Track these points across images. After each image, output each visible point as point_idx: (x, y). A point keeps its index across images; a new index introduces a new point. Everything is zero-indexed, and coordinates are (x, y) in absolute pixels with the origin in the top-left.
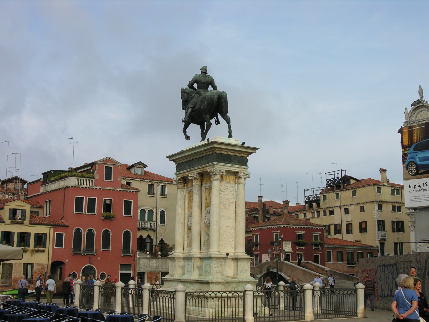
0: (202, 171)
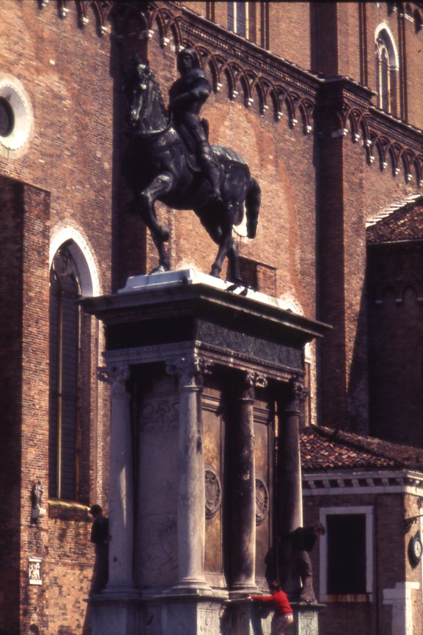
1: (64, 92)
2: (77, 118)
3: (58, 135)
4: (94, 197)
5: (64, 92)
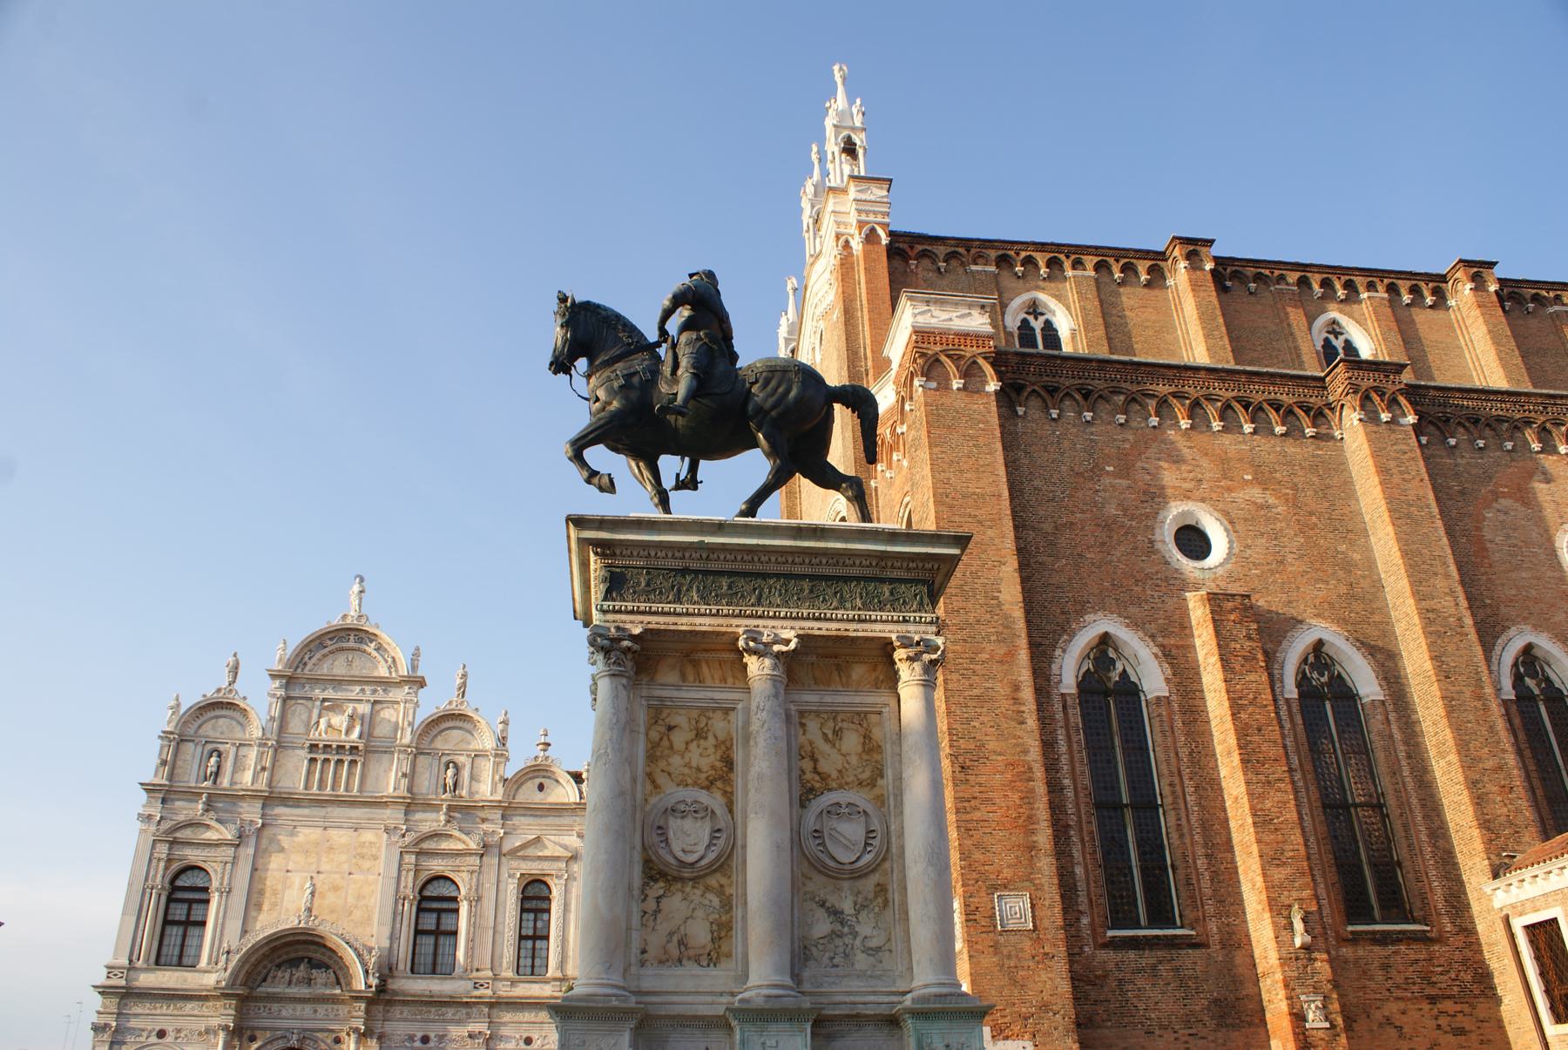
0: (834, 633)
1: (1271, 501)
2: (1298, 521)
3: (1274, 542)
4: (1345, 591)
5: (1271, 501)
